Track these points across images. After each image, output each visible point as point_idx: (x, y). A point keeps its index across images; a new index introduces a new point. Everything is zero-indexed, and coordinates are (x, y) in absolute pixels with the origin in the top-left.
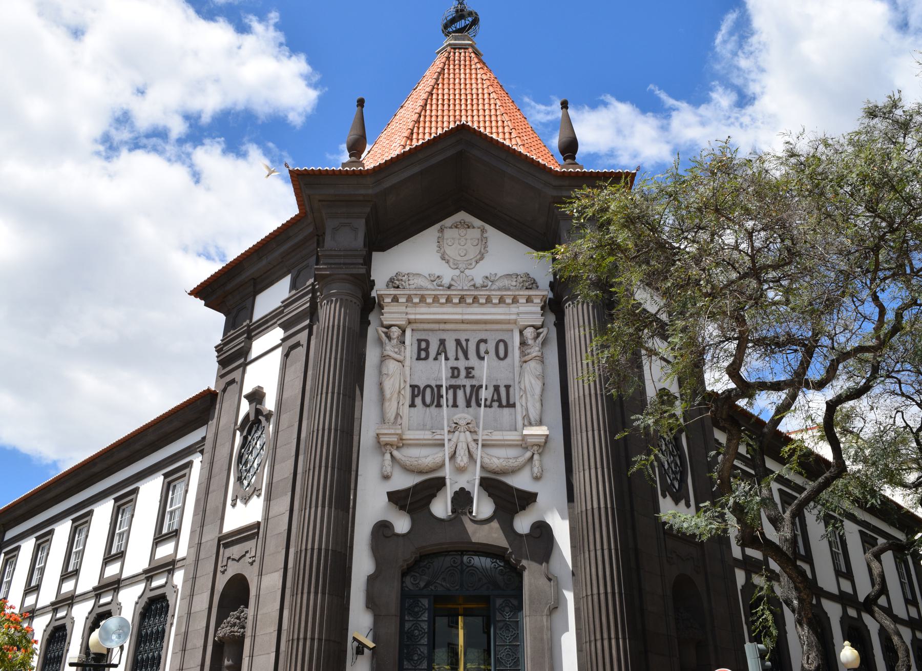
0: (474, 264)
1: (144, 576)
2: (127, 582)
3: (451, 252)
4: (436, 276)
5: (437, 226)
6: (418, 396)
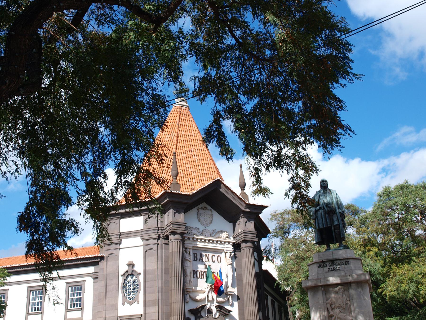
3: (202, 219)
4: (197, 227)
5: (196, 208)
6: (195, 274)
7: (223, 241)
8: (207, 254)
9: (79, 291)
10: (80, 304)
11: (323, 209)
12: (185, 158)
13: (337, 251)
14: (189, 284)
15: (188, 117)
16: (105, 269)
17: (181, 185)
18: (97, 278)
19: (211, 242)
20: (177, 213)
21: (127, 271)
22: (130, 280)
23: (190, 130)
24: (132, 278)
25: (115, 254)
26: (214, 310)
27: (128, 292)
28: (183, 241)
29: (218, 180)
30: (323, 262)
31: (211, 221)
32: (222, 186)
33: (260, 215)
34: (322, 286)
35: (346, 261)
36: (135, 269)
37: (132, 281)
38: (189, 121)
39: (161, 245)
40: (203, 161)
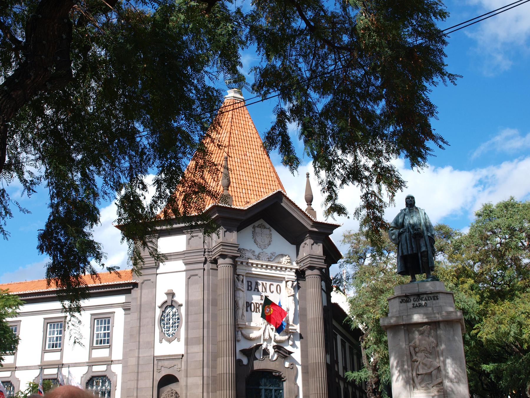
0: (267, 246)
3: (258, 239)
5: (252, 225)
6: (248, 306)
7: (284, 267)
8: (264, 282)
9: (107, 325)
10: (108, 340)
11: (408, 232)
12: (239, 163)
13: (423, 283)
14: (241, 319)
15: (243, 113)
16: (139, 299)
17: (234, 197)
18: (129, 309)
19: (269, 267)
20: (228, 232)
21: (166, 302)
22: (169, 313)
23: (246, 129)
24: (172, 311)
25: (152, 280)
26: (272, 351)
27: (167, 327)
28: (234, 266)
29: (280, 192)
30: (406, 296)
31: (270, 242)
32: (284, 199)
33: (330, 236)
34: (404, 325)
35: (434, 296)
36: (175, 299)
37: (171, 314)
38: (244, 118)
39: (208, 271)
40: (260, 167)
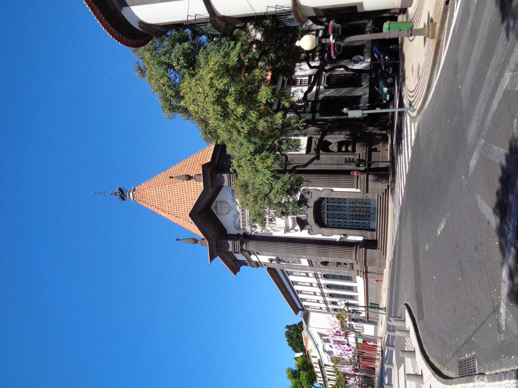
1: (318, 279)
2: (319, 282)
5: (217, 215)
